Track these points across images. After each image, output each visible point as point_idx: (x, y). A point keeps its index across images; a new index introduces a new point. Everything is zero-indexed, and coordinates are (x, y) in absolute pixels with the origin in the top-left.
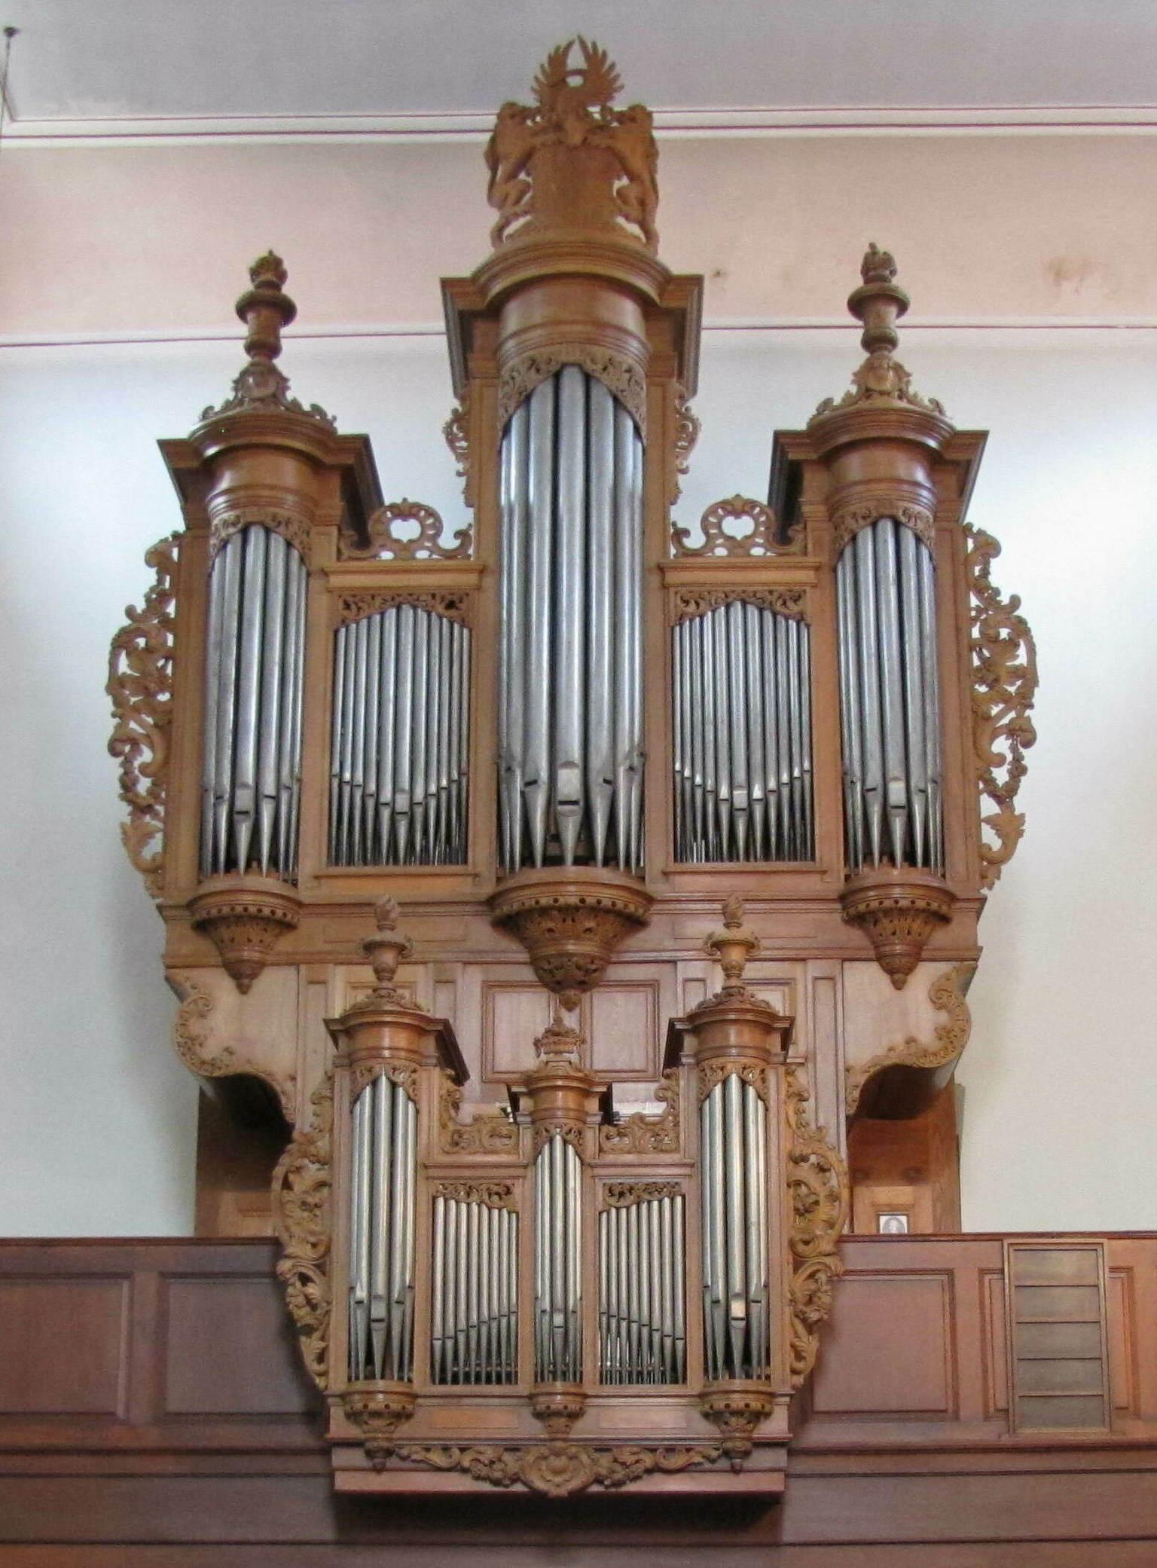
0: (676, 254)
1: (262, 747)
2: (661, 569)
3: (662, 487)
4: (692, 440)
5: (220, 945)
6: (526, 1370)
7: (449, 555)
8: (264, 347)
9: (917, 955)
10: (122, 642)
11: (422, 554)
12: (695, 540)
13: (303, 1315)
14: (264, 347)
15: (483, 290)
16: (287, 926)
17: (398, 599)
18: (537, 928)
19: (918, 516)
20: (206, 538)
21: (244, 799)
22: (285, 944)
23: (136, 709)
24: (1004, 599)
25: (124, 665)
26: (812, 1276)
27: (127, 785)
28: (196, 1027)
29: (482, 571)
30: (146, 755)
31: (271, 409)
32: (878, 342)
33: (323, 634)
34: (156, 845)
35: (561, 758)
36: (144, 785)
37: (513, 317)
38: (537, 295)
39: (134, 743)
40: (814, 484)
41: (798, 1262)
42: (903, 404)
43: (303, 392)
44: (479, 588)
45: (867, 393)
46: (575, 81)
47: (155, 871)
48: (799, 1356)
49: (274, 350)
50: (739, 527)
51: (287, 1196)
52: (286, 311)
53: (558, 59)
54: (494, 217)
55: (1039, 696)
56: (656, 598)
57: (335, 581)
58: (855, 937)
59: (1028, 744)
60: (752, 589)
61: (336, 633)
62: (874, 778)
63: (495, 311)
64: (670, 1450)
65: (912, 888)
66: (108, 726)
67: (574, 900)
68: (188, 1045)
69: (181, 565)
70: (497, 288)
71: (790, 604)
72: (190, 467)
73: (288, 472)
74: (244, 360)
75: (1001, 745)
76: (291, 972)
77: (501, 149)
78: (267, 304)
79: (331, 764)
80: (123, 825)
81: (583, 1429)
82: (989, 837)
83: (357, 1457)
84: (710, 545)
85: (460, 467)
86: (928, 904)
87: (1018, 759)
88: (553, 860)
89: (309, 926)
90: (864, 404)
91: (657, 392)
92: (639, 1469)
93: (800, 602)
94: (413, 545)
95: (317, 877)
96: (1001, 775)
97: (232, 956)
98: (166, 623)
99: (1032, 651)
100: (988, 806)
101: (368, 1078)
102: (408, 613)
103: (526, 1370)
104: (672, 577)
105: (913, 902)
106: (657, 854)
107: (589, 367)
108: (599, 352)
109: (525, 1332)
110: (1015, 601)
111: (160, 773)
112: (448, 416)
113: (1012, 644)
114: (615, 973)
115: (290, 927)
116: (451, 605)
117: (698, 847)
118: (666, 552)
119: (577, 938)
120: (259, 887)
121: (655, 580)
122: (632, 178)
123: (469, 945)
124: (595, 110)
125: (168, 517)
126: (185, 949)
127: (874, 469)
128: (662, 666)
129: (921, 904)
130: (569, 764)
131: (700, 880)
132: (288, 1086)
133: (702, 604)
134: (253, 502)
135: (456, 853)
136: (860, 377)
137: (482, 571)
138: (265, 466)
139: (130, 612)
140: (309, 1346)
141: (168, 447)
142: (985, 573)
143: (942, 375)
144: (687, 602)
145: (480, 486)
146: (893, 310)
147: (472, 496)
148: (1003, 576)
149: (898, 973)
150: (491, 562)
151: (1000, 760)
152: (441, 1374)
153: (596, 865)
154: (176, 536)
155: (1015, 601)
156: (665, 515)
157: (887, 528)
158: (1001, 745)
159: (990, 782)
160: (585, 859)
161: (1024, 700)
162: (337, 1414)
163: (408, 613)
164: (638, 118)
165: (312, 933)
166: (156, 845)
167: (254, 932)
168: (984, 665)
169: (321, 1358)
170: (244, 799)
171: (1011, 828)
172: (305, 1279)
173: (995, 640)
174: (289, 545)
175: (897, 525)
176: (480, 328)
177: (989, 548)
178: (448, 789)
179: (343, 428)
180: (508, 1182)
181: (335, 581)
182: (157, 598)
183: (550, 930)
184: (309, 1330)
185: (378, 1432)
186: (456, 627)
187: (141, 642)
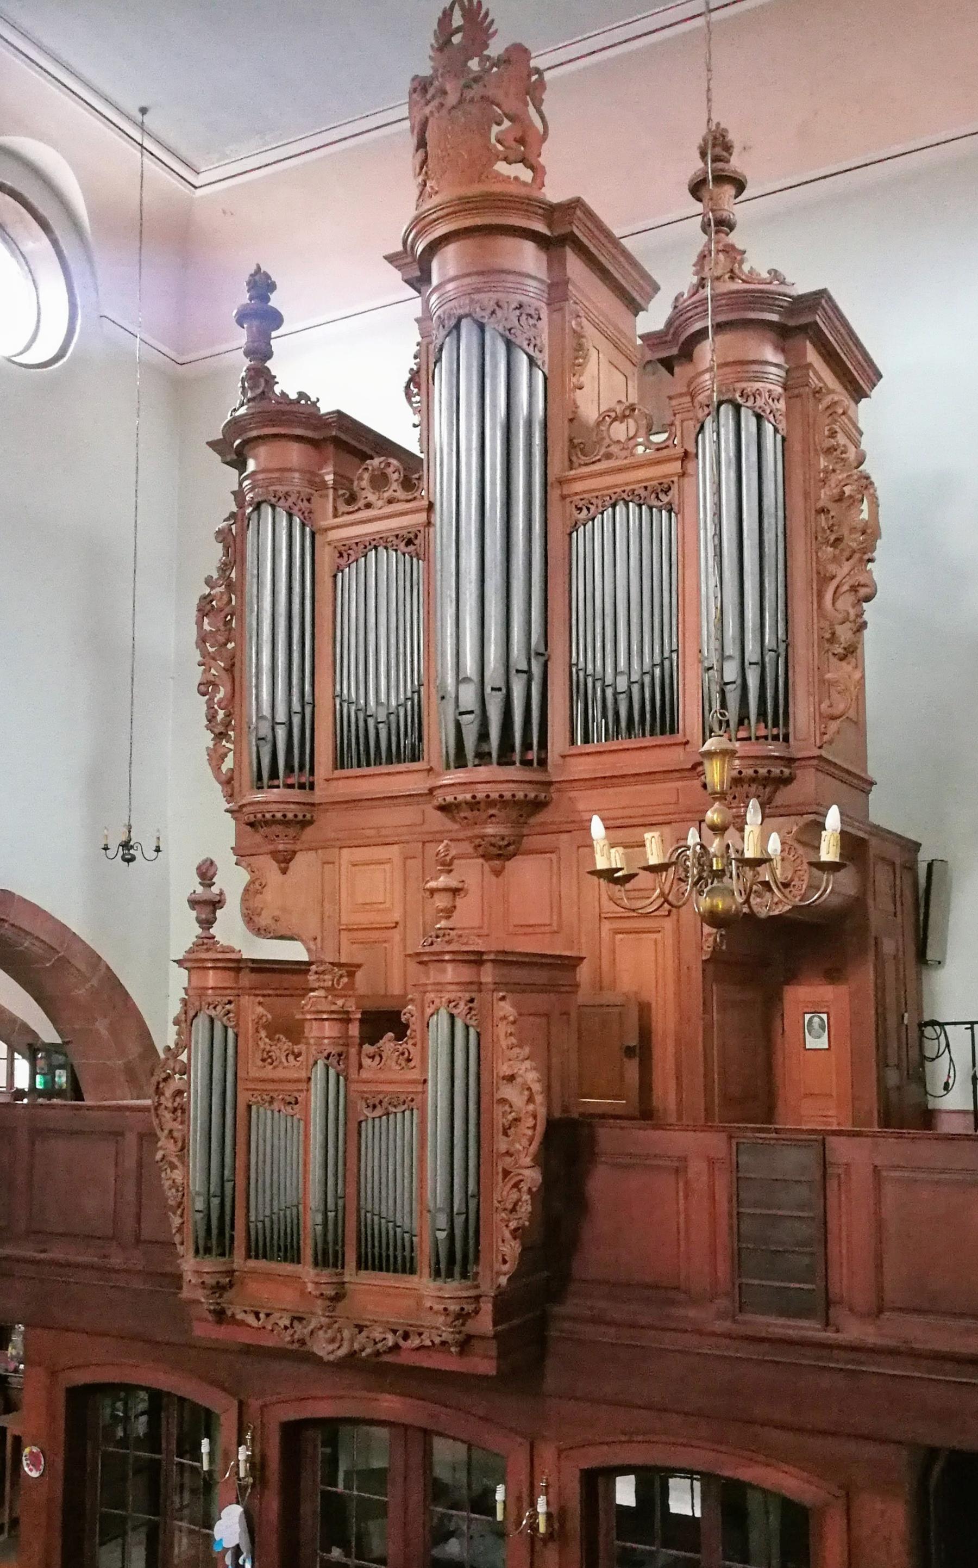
16: (305, 824)
22: (309, 832)
26: (516, 1185)
27: (211, 718)
28: (257, 902)
31: (264, 405)
42: (738, 285)
43: (288, 382)
47: (228, 782)
49: (268, 355)
52: (276, 319)
55: (881, 551)
57: (334, 535)
59: (868, 599)
60: (628, 488)
61: (335, 576)
66: (197, 674)
71: (662, 496)
76: (312, 854)
79: (334, 686)
80: (208, 748)
86: (756, 772)
93: (671, 493)
95: (327, 780)
99: (874, 504)
102: (383, 552)
105: (740, 773)
107: (478, 314)
113: (855, 501)
114: (527, 843)
115: (311, 822)
116: (409, 542)
123: (426, 828)
126: (247, 843)
133: (593, 508)
144: (580, 509)
146: (729, 190)
153: (491, 763)
157: (726, 412)
161: (865, 554)
163: (383, 552)
166: (228, 763)
175: (737, 408)
178: (412, 699)
179: (325, 408)
180: (296, 1094)
181: (334, 535)
183: (466, 818)
186: (415, 560)
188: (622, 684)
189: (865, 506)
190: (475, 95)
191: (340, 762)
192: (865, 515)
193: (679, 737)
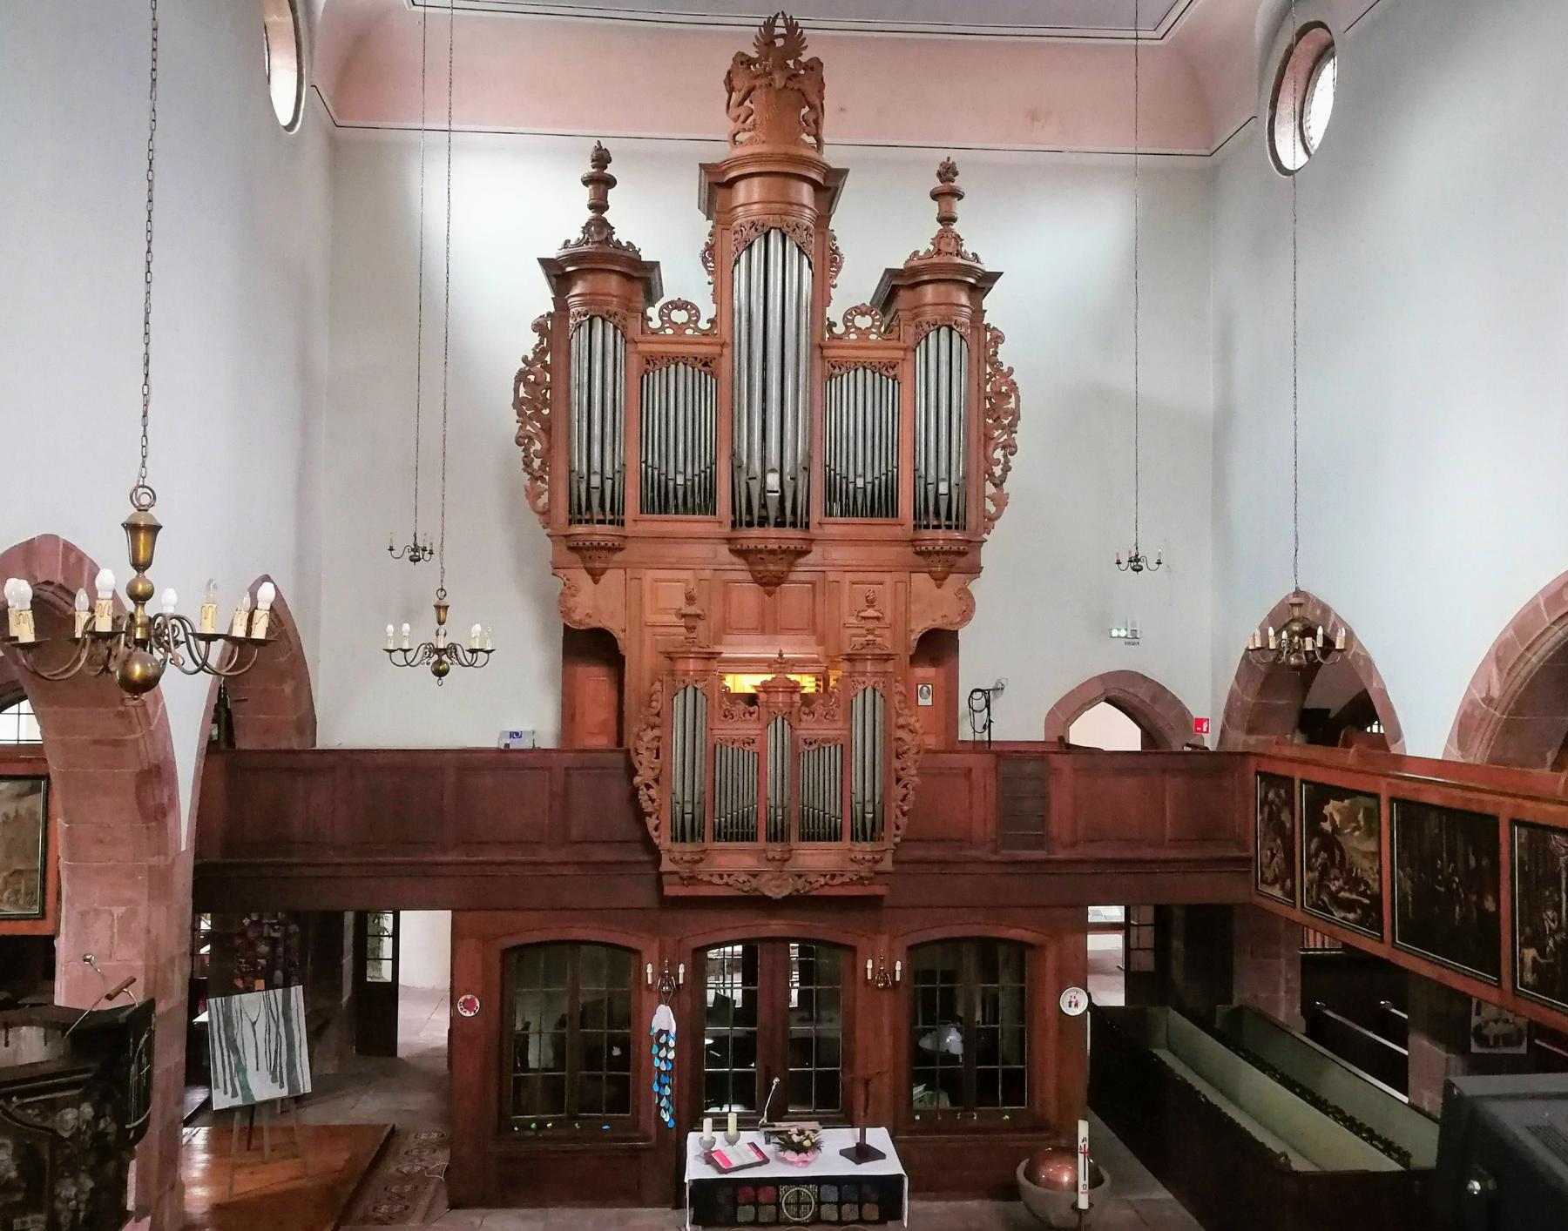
0: (832, 156)
1: (605, 455)
2: (821, 348)
3: (822, 296)
4: (839, 268)
5: (583, 559)
6: (762, 834)
7: (705, 334)
8: (599, 206)
9: (951, 569)
10: (521, 377)
11: (689, 332)
12: (839, 330)
13: (647, 806)
14: (599, 206)
15: (724, 173)
17: (675, 359)
18: (752, 557)
19: (960, 325)
20: (567, 317)
21: (595, 481)
22: (618, 557)
23: (530, 418)
24: (1005, 369)
25: (522, 393)
27: (527, 464)
28: (571, 603)
29: (722, 345)
30: (538, 446)
32: (947, 220)
33: (636, 383)
34: (545, 499)
35: (768, 467)
36: (537, 463)
37: (742, 192)
38: (756, 181)
39: (530, 439)
40: (904, 297)
41: (898, 780)
44: (721, 355)
45: (939, 252)
46: (780, 42)
47: (546, 514)
48: (898, 828)
50: (863, 322)
51: (639, 743)
53: (770, 25)
54: (732, 126)
56: (818, 362)
57: (640, 347)
58: (921, 560)
62: (931, 478)
63: (731, 183)
64: (833, 877)
65: (946, 534)
67: (775, 547)
68: (566, 613)
69: (552, 331)
70: (733, 174)
72: (559, 273)
73: (613, 284)
74: (590, 214)
75: (999, 454)
77: (736, 83)
78: (600, 182)
81: (788, 867)
82: (991, 507)
83: (676, 879)
84: (847, 332)
85: (710, 279)
87: (1007, 462)
88: (763, 522)
89: (631, 546)
90: (936, 259)
91: (820, 238)
92: (816, 885)
94: (685, 325)
96: (998, 471)
97: (589, 565)
98: (546, 367)
100: (990, 489)
101: (682, 686)
103: (762, 834)
104: (827, 352)
106: (816, 515)
107: (785, 229)
108: (790, 219)
109: (762, 814)
110: (1011, 370)
111: (546, 455)
112: (703, 247)
114: (793, 576)
116: (705, 365)
117: (836, 508)
118: (823, 338)
119: (775, 563)
120: (602, 532)
121: (818, 352)
122: (812, 107)
124: (791, 63)
125: (543, 301)
127: (939, 290)
128: (818, 408)
129: (954, 548)
130: (773, 471)
131: (838, 527)
132: (622, 635)
134: (593, 303)
135: (707, 504)
136: (937, 241)
137: (722, 345)
138: (599, 272)
139: (525, 360)
140: (651, 822)
141: (546, 263)
142: (996, 353)
143: (982, 241)
145: (722, 290)
147: (717, 298)
148: (1005, 354)
149: (939, 580)
150: (728, 340)
151: (998, 462)
152: (719, 835)
154: (549, 314)
155: (1011, 370)
156: (824, 313)
157: (944, 331)
158: (999, 454)
159: (992, 475)
160: (780, 524)
161: (1011, 429)
162: (665, 858)
164: (815, 66)
165: (633, 552)
166: (545, 499)
167: (603, 554)
168: (993, 408)
169: (656, 829)
170: (595, 481)
171: (1001, 502)
172: (648, 787)
173: (999, 393)
174: (615, 328)
175: (951, 329)
176: (721, 192)
177: (998, 339)
181: (640, 347)
182: (540, 353)
184: (650, 815)
185: (685, 871)
187: (532, 378)
188: (860, 483)
189: (1013, 400)
190: (780, 77)
191: (647, 506)
192: (1012, 405)
193: (899, 521)
